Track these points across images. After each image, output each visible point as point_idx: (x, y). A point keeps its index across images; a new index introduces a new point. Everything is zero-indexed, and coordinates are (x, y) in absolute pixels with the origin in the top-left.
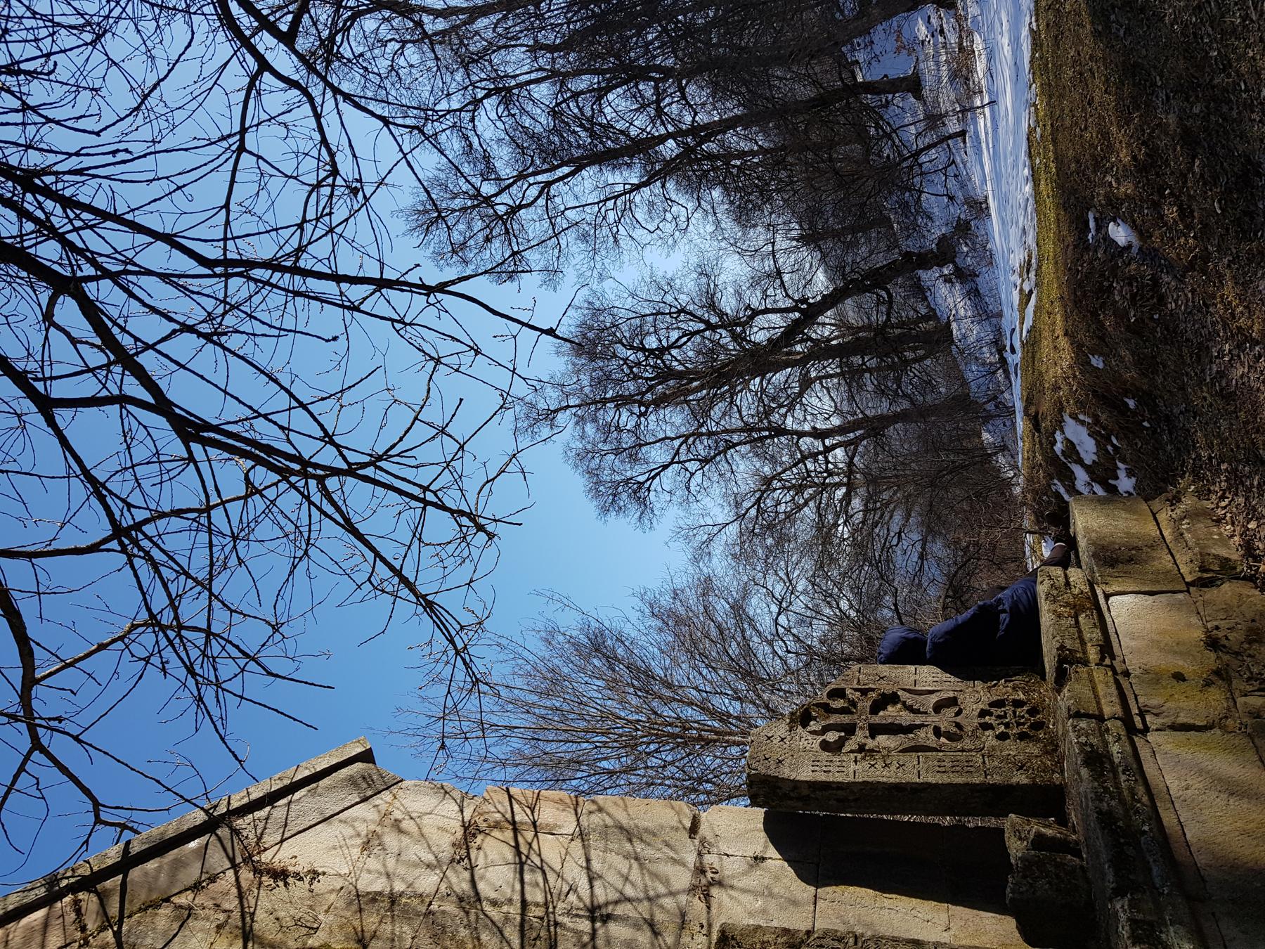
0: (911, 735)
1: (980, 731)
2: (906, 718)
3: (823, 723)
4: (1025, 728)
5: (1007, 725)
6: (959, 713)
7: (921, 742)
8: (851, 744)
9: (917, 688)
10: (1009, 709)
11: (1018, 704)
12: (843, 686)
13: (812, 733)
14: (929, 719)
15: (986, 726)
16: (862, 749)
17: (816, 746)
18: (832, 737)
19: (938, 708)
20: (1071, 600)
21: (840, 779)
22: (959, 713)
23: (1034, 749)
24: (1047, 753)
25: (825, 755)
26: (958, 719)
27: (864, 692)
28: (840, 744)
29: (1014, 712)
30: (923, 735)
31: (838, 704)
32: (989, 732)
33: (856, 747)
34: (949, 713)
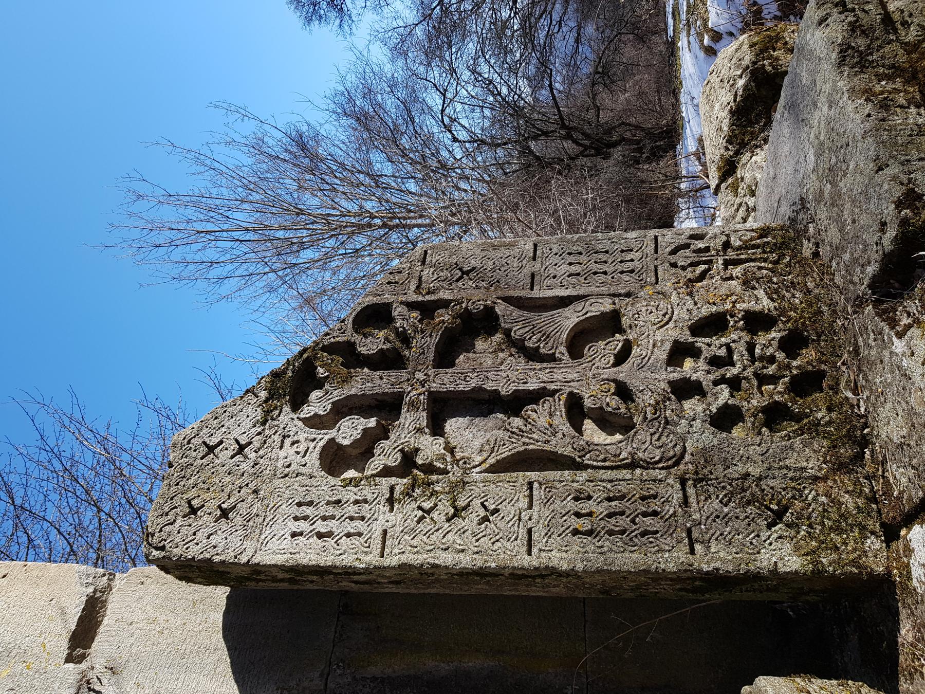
0: (517, 422)
1: (672, 404)
2: (510, 375)
3: (337, 395)
4: (777, 392)
5: (734, 384)
6: (622, 357)
7: (536, 442)
8: (386, 455)
9: (537, 293)
10: (736, 337)
11: (757, 322)
12: (388, 298)
13: (314, 422)
14: (558, 375)
15: (685, 389)
16: (408, 460)
17: (313, 459)
18: (349, 430)
19: (577, 343)
20: (902, 58)
21: (348, 560)
22: (622, 357)
23: (809, 457)
24: (840, 467)
25: (326, 486)
26: (623, 372)
27: (427, 310)
28: (365, 447)
29: (751, 347)
30: (543, 421)
31: (373, 343)
32: (692, 406)
33: (393, 460)
34: (602, 351)
